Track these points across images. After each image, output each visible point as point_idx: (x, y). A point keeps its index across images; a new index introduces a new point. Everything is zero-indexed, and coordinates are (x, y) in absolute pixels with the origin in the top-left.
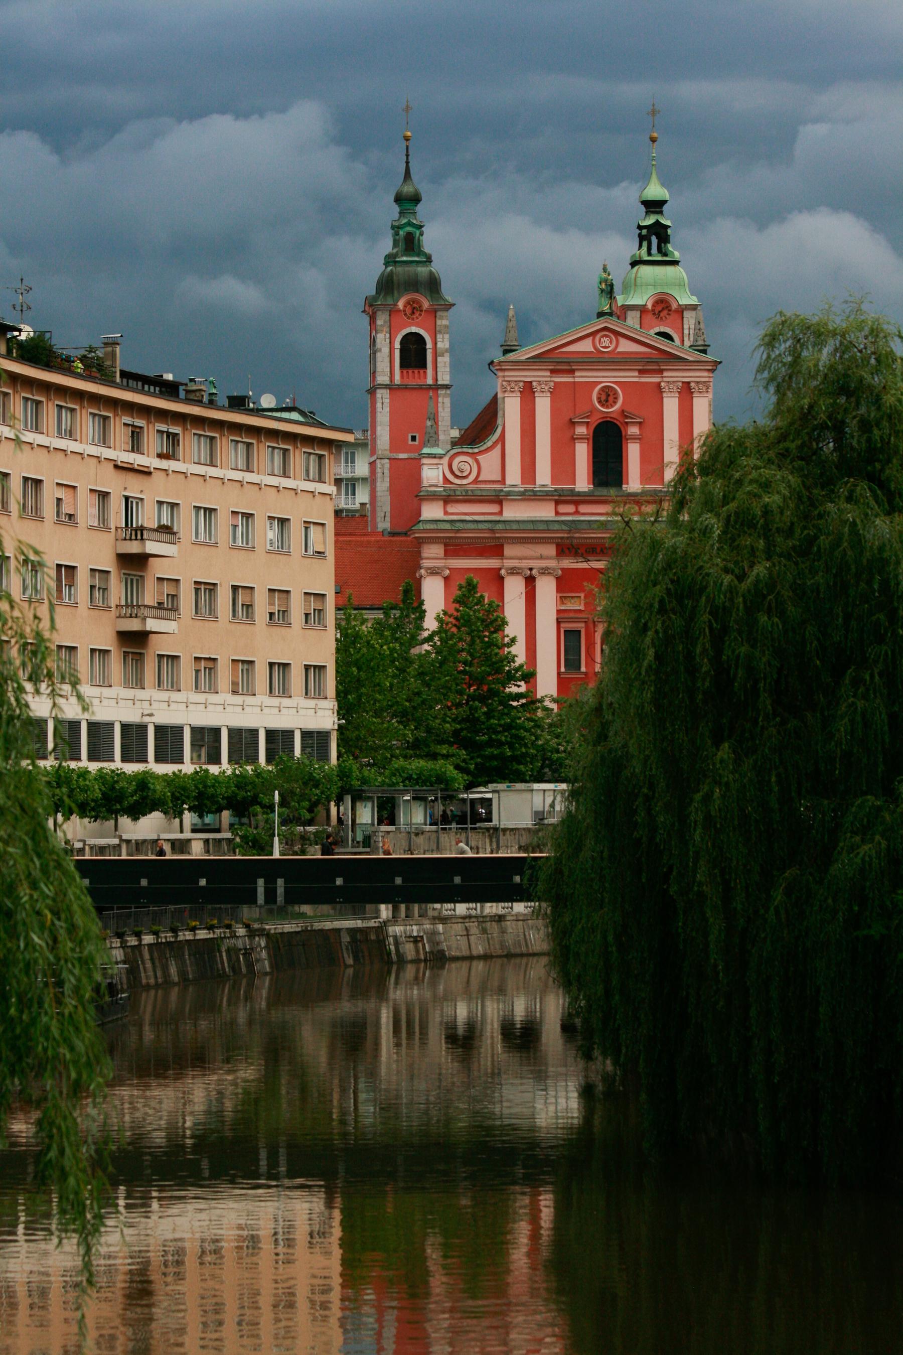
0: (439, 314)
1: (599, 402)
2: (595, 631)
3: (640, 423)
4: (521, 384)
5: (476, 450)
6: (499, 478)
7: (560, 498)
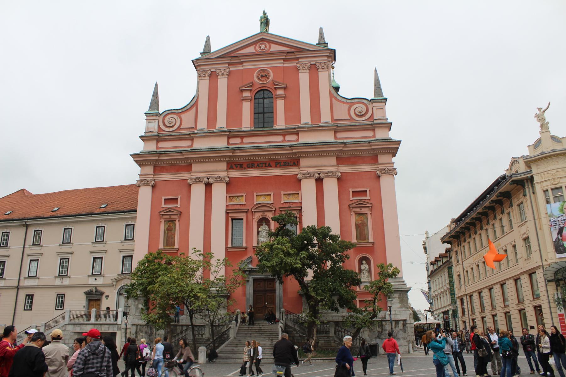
1: (259, 79)
2: (253, 218)
3: (285, 88)
4: (209, 72)
6: (193, 126)
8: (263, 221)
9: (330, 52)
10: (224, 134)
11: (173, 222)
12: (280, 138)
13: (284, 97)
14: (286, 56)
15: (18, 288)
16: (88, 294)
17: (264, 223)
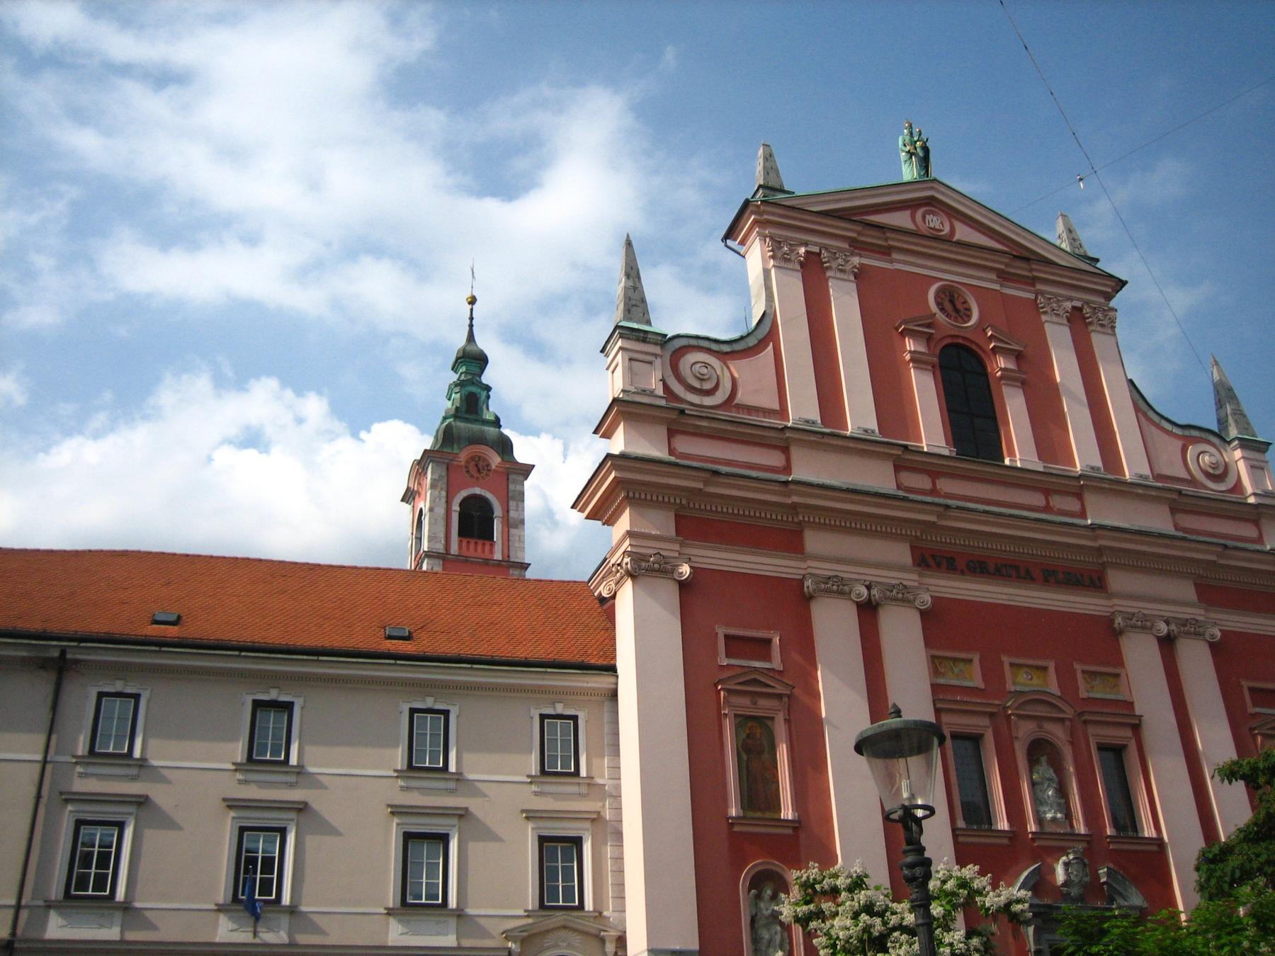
0: (512, 477)
1: (942, 310)
5: (726, 348)
9: (1113, 284)
10: (887, 451)
11: (763, 722)
12: (1037, 499)
14: (1007, 265)
17: (1044, 759)
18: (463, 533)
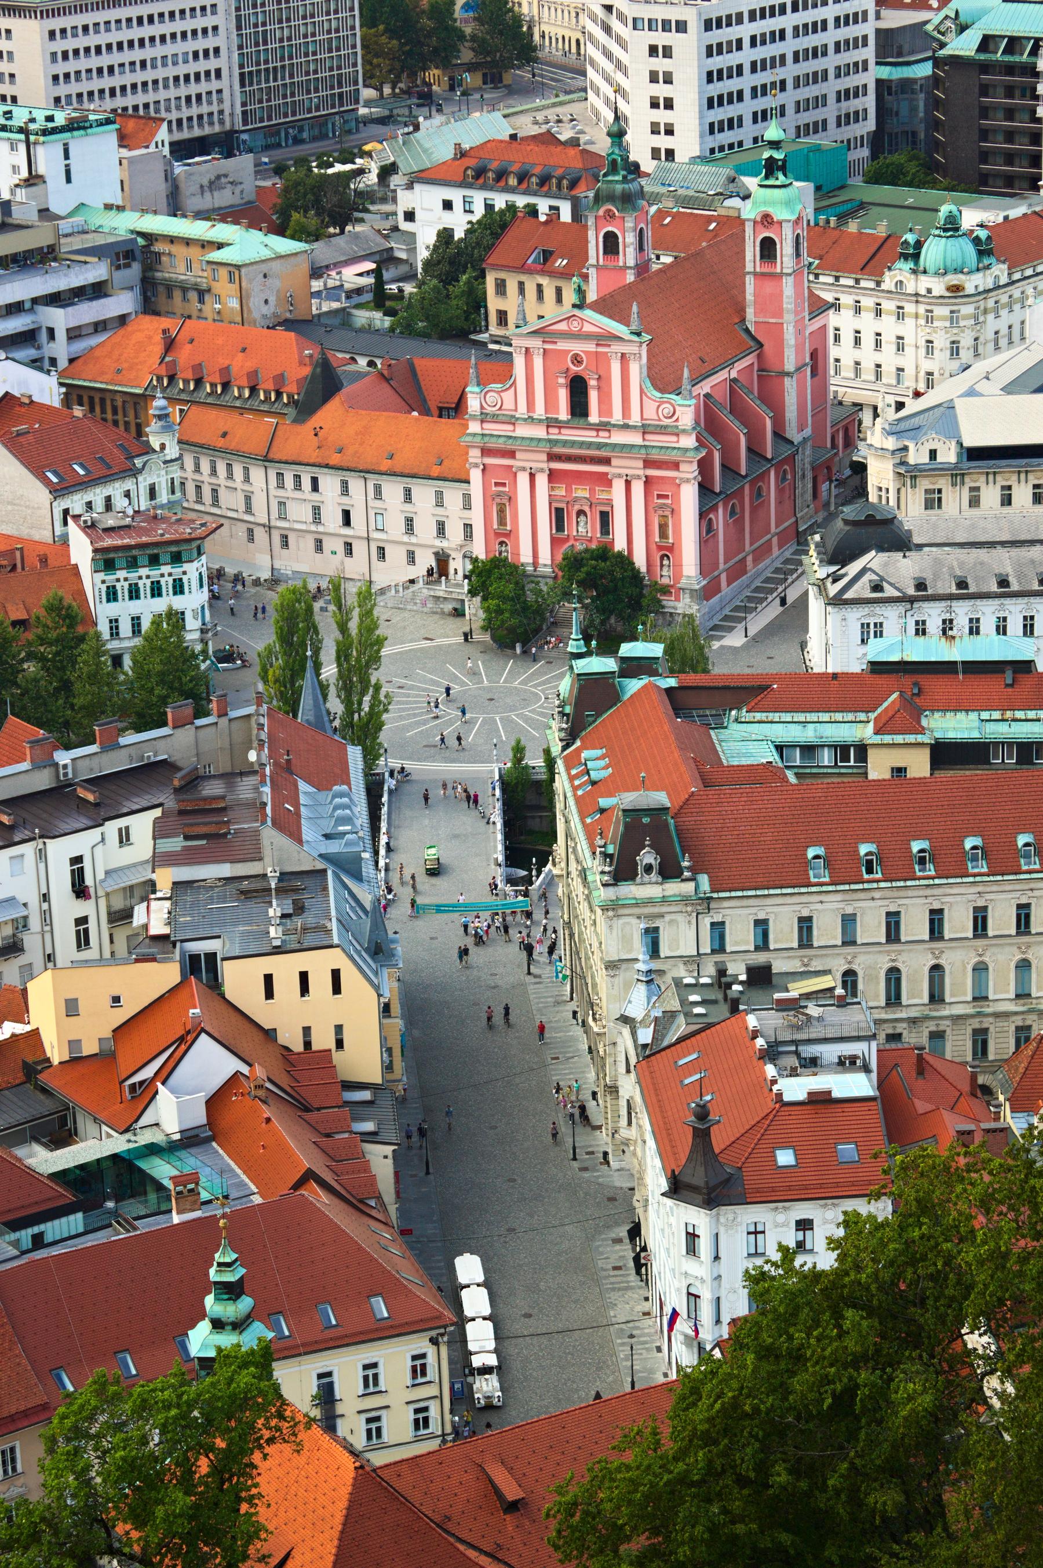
7: (551, 423)
8: (581, 513)
12: (594, 433)
13: (599, 388)
15: (368, 539)
16: (436, 554)
18: (605, 252)
